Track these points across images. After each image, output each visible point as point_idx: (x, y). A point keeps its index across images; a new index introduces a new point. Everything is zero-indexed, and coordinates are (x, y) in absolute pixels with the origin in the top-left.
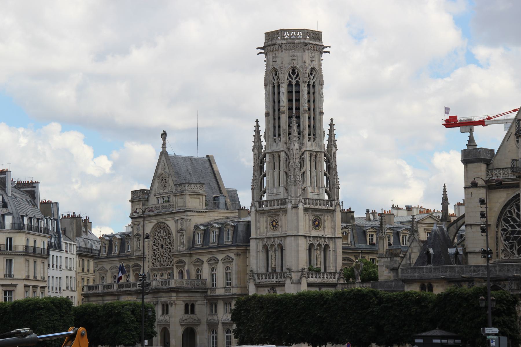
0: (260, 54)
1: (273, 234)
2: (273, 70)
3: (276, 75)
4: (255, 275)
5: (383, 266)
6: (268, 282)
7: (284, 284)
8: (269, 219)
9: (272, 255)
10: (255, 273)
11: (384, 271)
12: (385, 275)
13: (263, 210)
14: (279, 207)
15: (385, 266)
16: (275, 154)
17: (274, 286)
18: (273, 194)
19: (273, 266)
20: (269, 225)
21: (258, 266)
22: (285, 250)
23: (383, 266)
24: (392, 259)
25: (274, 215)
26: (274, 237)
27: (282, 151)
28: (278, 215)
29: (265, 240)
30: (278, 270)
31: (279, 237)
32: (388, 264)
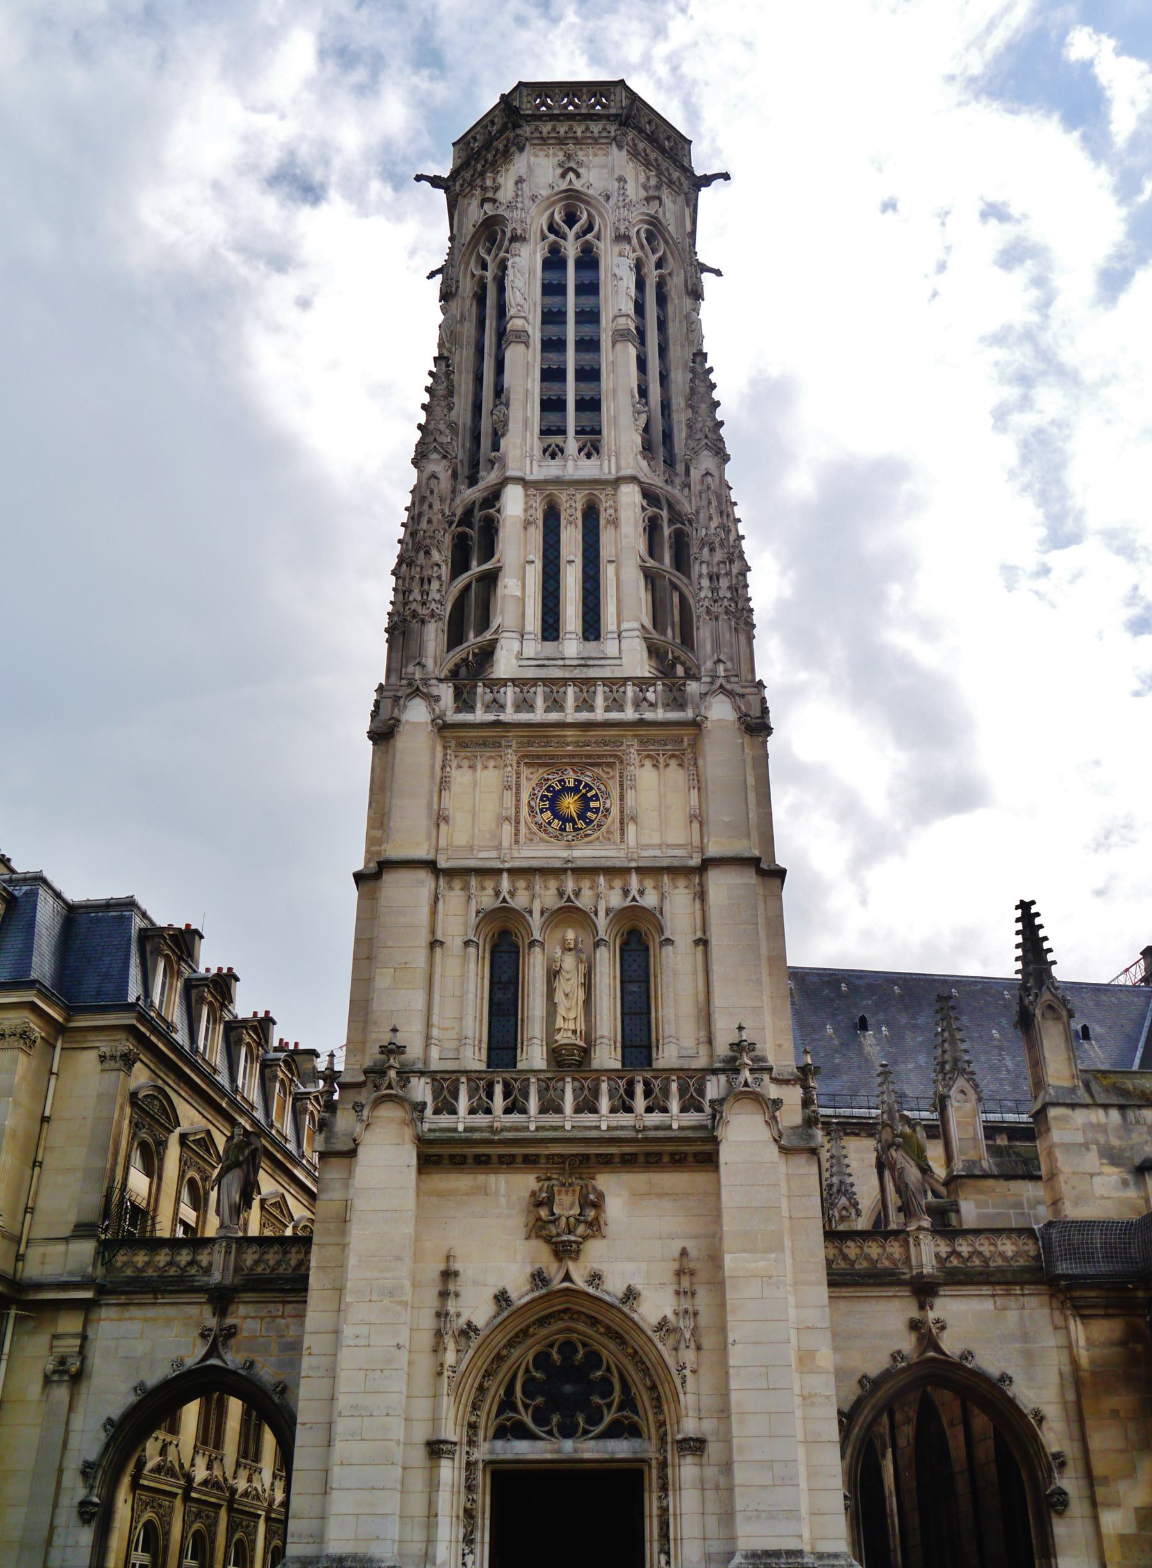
0: (426, 185)
1: (565, 854)
2: (561, 200)
3: (571, 220)
4: (414, 1080)
5: (1086, 1146)
6: (538, 1129)
7: (708, 1147)
8: (530, 781)
9: (553, 974)
10: (419, 1066)
11: (1092, 1175)
12: (1102, 1197)
13: (497, 724)
14: (630, 714)
15: (1094, 1147)
16: (563, 497)
17: (586, 1157)
18: (561, 662)
19: (563, 1038)
20: (524, 811)
21: (435, 1032)
22: (669, 941)
23: (1086, 1146)
24: (1131, 1114)
25: (573, 756)
26: (580, 872)
27: (633, 479)
28: (613, 761)
29: (505, 883)
30: (607, 1057)
31: (624, 871)
32: (1115, 1142)
